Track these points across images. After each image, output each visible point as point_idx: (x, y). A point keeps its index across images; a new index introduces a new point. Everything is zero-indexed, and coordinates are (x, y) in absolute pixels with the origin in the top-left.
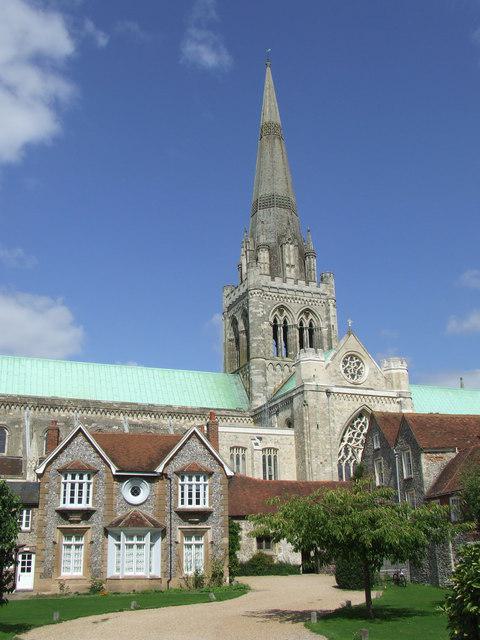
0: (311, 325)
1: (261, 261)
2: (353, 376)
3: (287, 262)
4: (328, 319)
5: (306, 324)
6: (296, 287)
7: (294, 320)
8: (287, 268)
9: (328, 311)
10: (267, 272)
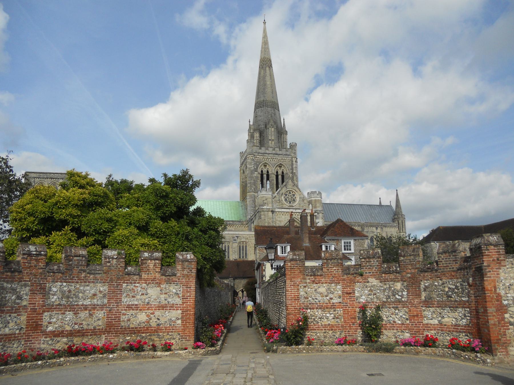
0: (283, 173)
1: (255, 138)
2: (290, 202)
3: (270, 138)
5: (280, 172)
6: (274, 152)
8: (270, 142)
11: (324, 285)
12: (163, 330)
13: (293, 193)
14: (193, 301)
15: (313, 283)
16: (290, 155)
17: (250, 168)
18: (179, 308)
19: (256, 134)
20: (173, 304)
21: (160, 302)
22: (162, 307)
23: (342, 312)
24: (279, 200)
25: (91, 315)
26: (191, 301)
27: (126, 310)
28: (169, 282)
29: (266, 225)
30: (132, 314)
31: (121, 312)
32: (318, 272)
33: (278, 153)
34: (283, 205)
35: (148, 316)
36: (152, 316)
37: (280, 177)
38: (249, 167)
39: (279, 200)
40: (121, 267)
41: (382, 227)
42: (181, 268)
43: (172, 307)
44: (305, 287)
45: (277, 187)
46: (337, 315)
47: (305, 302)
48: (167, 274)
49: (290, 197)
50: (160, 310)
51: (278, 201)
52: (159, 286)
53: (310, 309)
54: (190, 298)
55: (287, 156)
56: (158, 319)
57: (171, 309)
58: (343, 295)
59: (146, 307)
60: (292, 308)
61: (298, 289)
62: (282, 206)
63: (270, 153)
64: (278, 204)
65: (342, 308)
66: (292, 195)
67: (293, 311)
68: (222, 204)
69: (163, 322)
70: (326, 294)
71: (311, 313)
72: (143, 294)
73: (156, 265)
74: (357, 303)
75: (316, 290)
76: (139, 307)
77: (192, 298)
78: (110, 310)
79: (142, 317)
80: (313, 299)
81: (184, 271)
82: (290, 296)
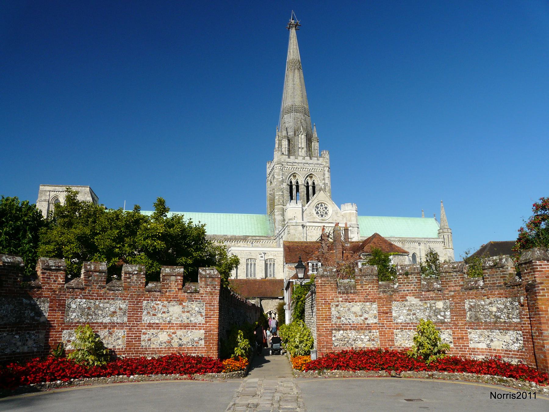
0: (314, 183)
2: (322, 216)
4: (324, 179)
6: (304, 161)
7: (301, 181)
9: (324, 174)
10: (287, 153)
11: (358, 304)
12: (185, 350)
13: (325, 206)
14: (216, 320)
15: (346, 302)
16: (321, 164)
17: (278, 179)
18: (202, 328)
19: (284, 141)
20: (196, 324)
21: (182, 321)
22: (185, 326)
23: (378, 333)
24: (310, 213)
25: (110, 333)
26: (214, 320)
27: (146, 329)
28: (191, 300)
29: (296, 240)
30: (153, 334)
31: (141, 331)
32: (351, 290)
33: (309, 162)
34: (314, 218)
35: (169, 335)
36: (173, 335)
37: (311, 188)
38: (277, 177)
39: (310, 213)
40: (142, 283)
41: (425, 242)
42: (204, 285)
43: (194, 326)
44: (337, 306)
45: (308, 200)
46: (373, 337)
47: (337, 322)
48: (189, 291)
49: (322, 210)
50: (181, 329)
51: (310, 215)
52: (181, 304)
53: (343, 330)
54: (213, 317)
55: (318, 165)
56: (180, 339)
57: (193, 329)
58: (379, 315)
59: (167, 326)
60: (323, 329)
61: (330, 308)
62: (313, 220)
63: (299, 162)
64: (308, 218)
65: (378, 329)
66: (324, 208)
67: (324, 332)
68: (247, 218)
69: (185, 343)
70: (360, 314)
71: (344, 335)
72: (164, 312)
73: (178, 282)
74: (394, 324)
75: (349, 309)
76: (160, 326)
77: (215, 317)
78: (130, 329)
79: (163, 337)
80: (346, 319)
81: (208, 287)
82: (321, 315)
